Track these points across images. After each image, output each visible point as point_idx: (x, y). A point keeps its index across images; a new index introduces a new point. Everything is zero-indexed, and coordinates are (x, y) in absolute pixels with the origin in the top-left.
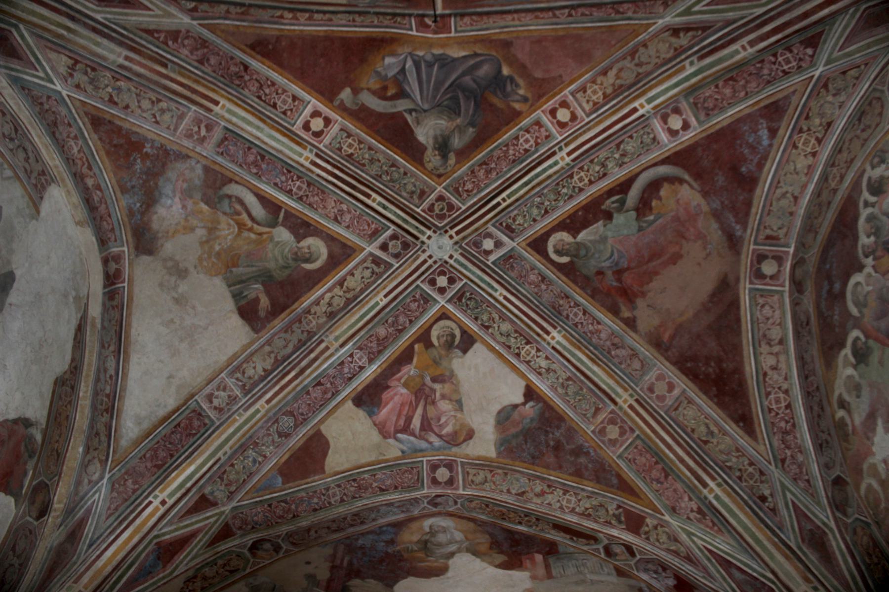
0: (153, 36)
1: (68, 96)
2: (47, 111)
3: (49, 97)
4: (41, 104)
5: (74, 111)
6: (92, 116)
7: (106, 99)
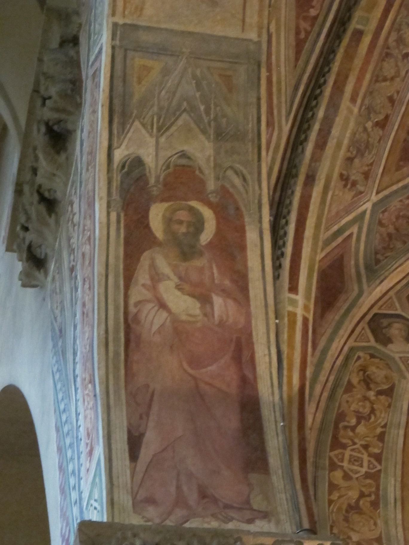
0: (304, 41)
1: (378, 193)
2: (397, 229)
3: (380, 223)
4: (390, 235)
5: (395, 188)
6: (401, 159)
7: (381, 132)
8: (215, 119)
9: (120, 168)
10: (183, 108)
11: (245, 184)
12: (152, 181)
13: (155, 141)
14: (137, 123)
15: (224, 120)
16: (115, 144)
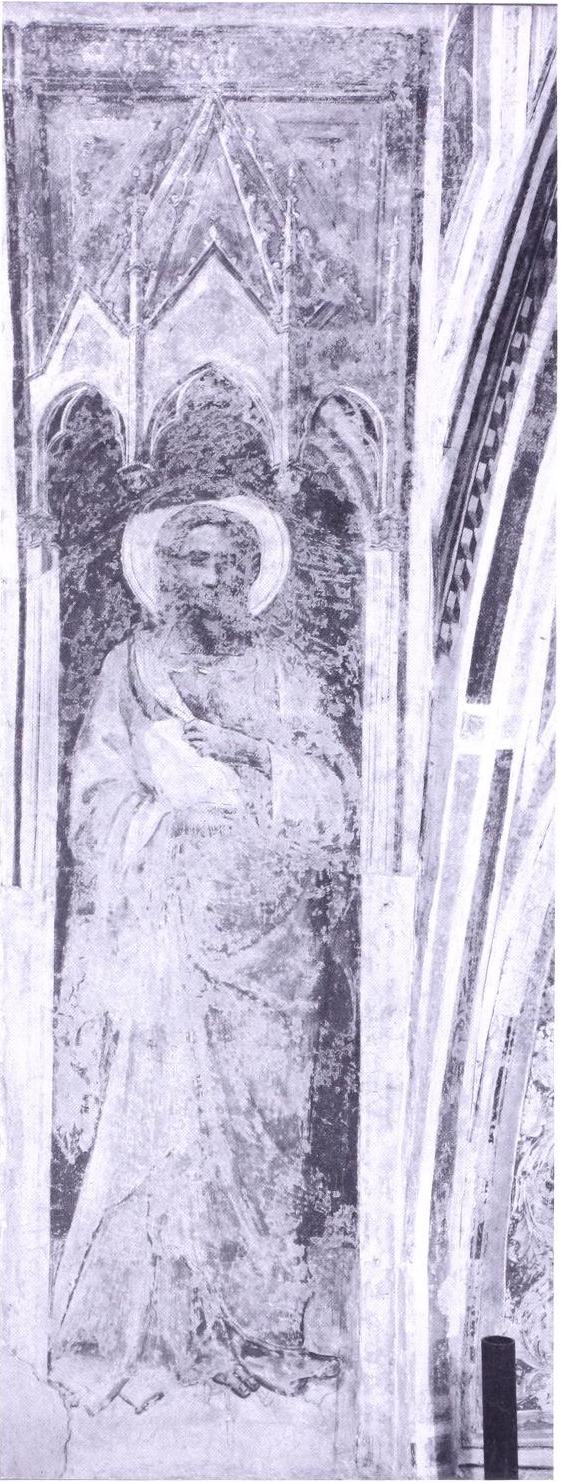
8: (294, 269)
9: (47, 428)
10: (208, 245)
11: (369, 438)
12: (130, 452)
13: (133, 347)
14: (86, 303)
15: (319, 269)
16: (32, 367)
